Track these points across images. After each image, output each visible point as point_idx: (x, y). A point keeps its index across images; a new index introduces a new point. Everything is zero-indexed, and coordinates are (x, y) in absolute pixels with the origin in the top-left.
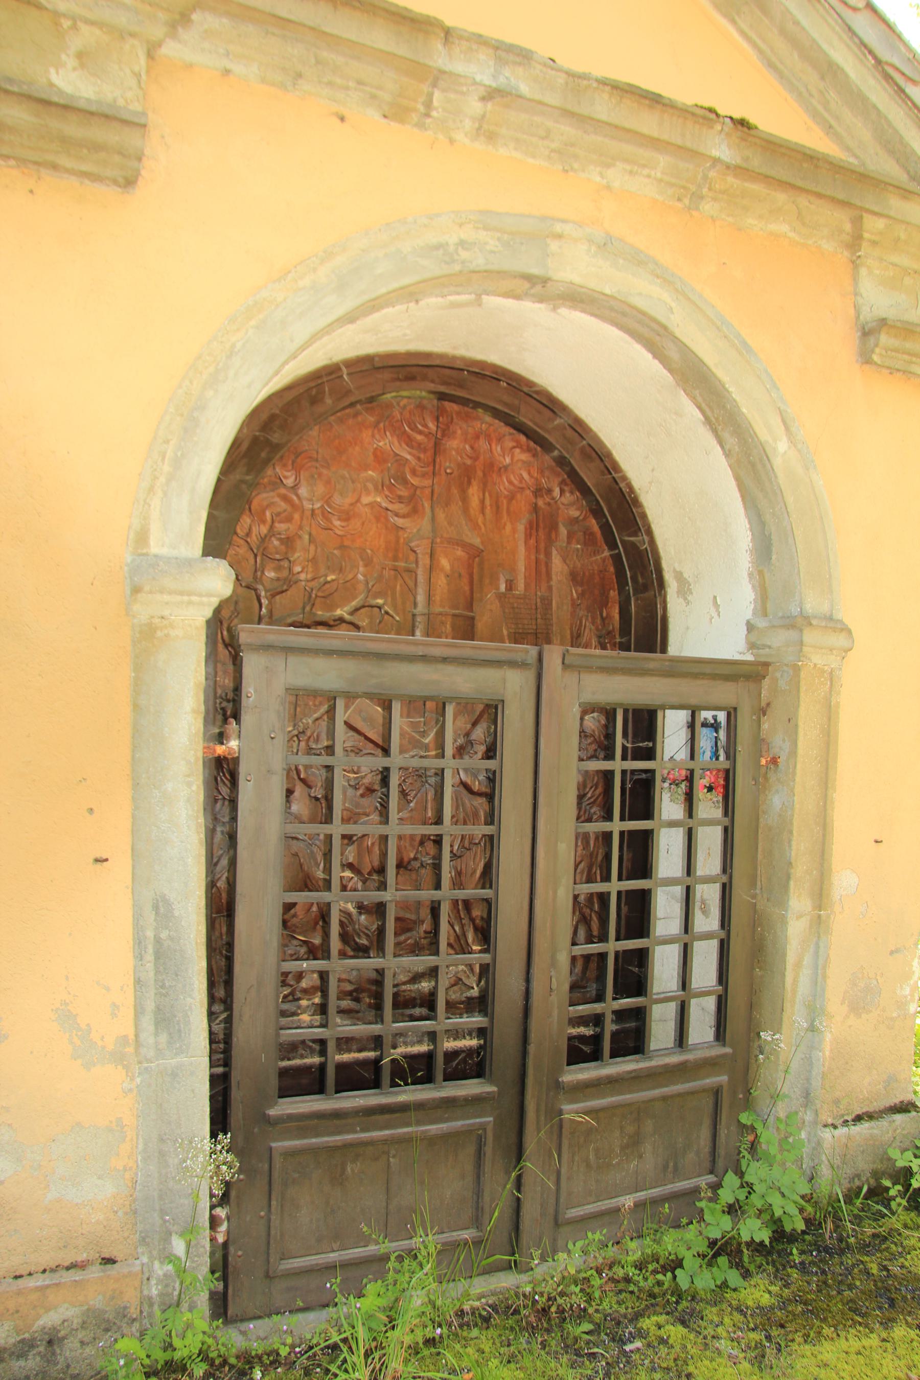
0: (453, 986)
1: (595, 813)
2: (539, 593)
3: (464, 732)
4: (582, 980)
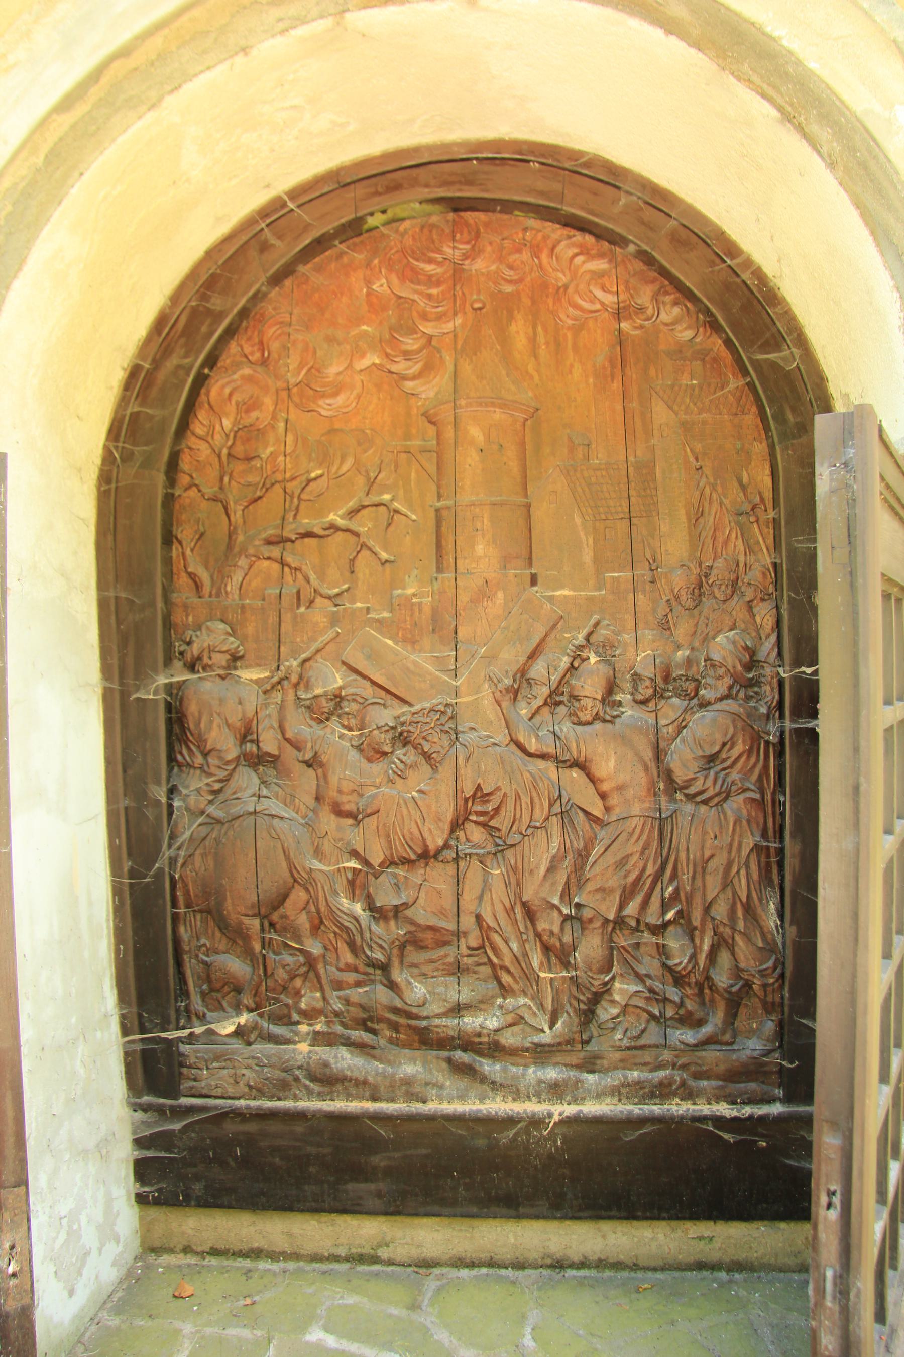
0: (510, 1025)
1: (733, 783)
2: (631, 459)
3: (515, 669)
4: (724, 1032)
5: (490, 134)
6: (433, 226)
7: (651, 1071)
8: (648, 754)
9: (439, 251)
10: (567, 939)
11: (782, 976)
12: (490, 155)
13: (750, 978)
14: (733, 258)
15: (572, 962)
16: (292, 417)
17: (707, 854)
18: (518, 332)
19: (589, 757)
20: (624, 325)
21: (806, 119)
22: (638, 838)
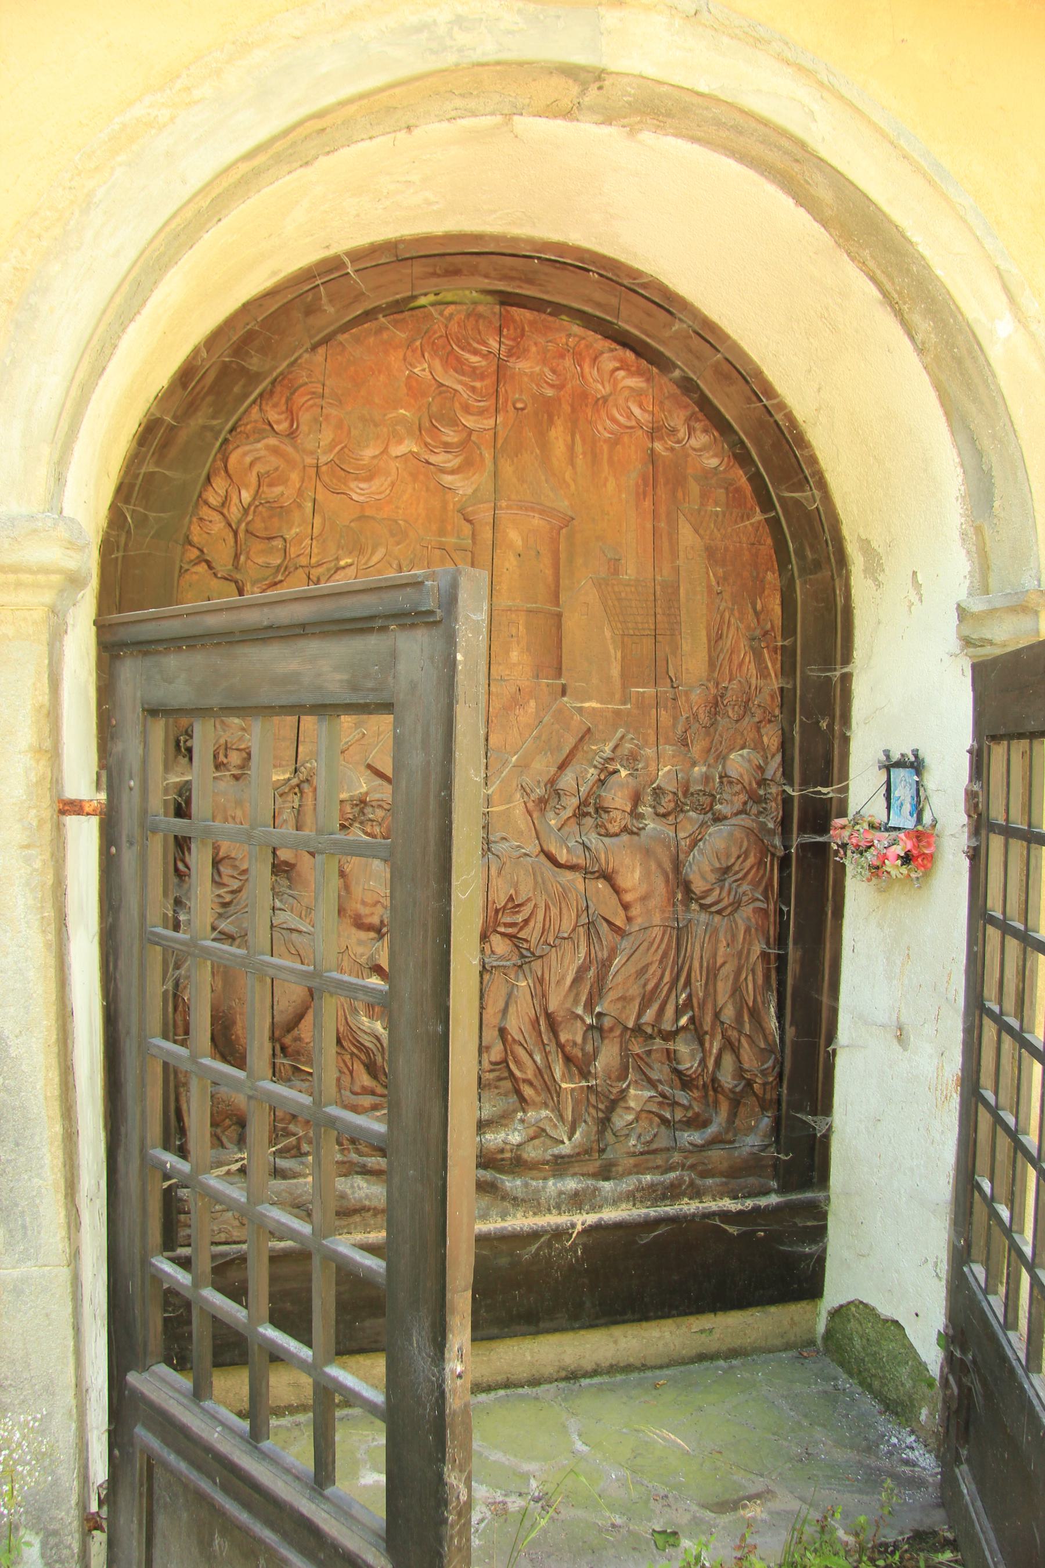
0: (532, 1139)
1: (744, 894)
2: (658, 578)
3: (546, 779)
4: (727, 1133)
5: (555, 237)
6: (480, 316)
7: (662, 1174)
8: (668, 866)
9: (484, 343)
10: (589, 1048)
11: (780, 1075)
12: (553, 258)
13: (753, 1077)
14: (769, 398)
15: (593, 1071)
16: (319, 497)
17: (719, 961)
18: (557, 438)
19: (616, 868)
20: (658, 446)
21: (909, 309)
22: (658, 947)
